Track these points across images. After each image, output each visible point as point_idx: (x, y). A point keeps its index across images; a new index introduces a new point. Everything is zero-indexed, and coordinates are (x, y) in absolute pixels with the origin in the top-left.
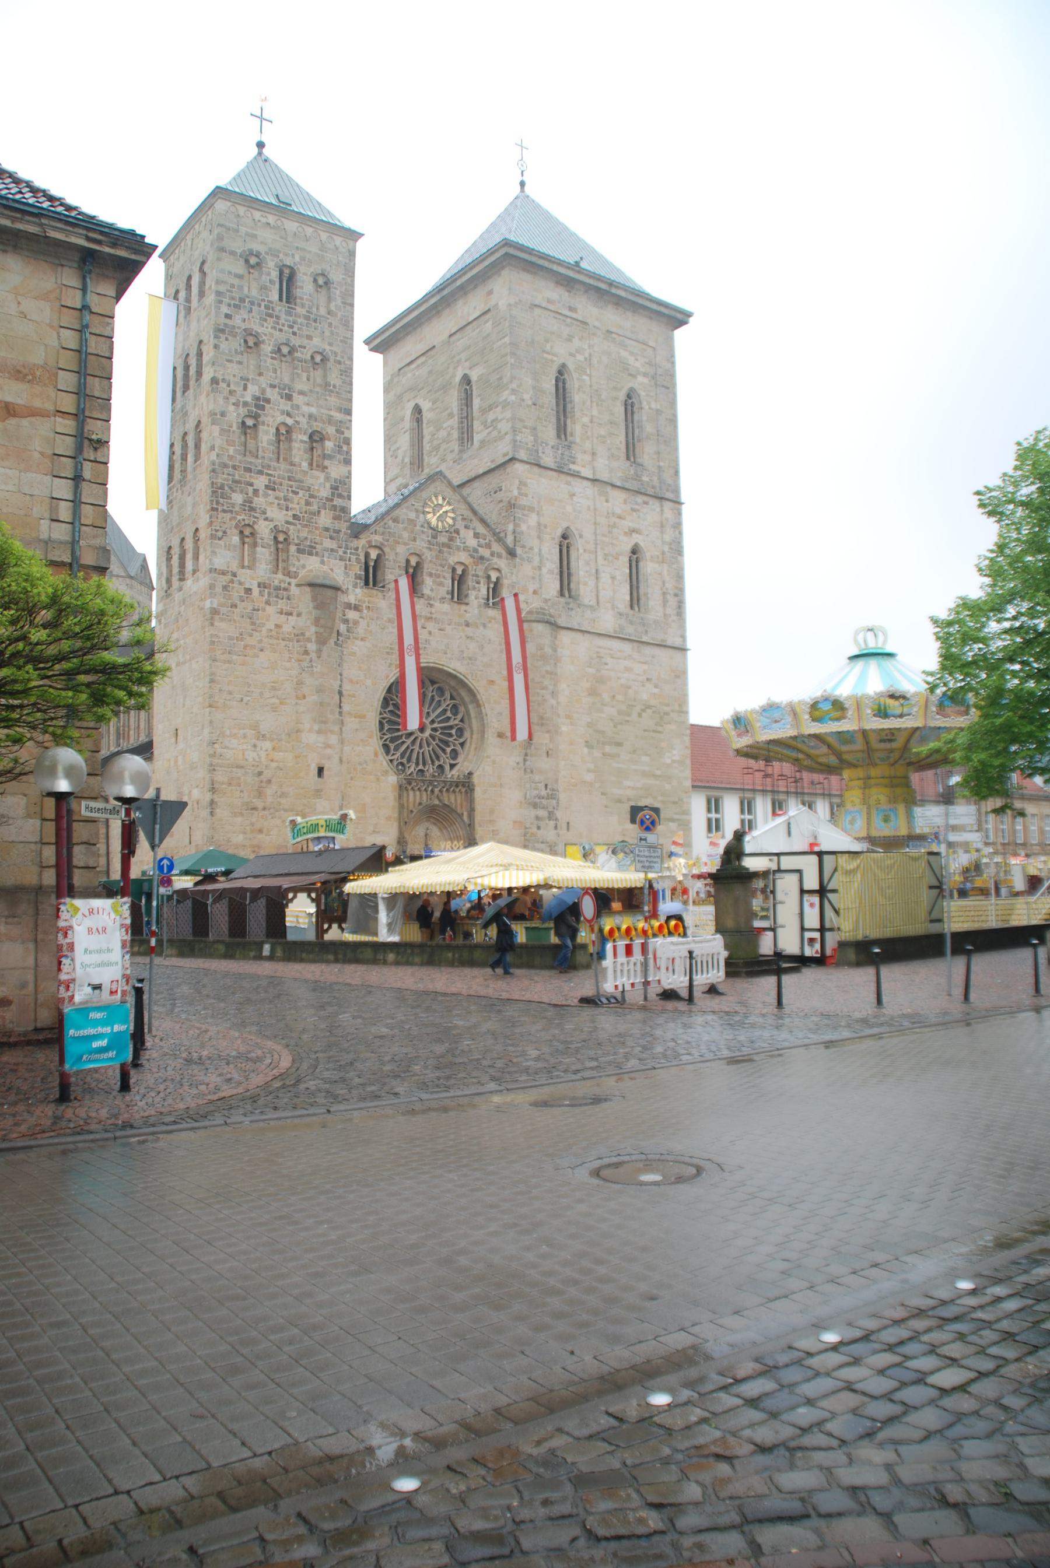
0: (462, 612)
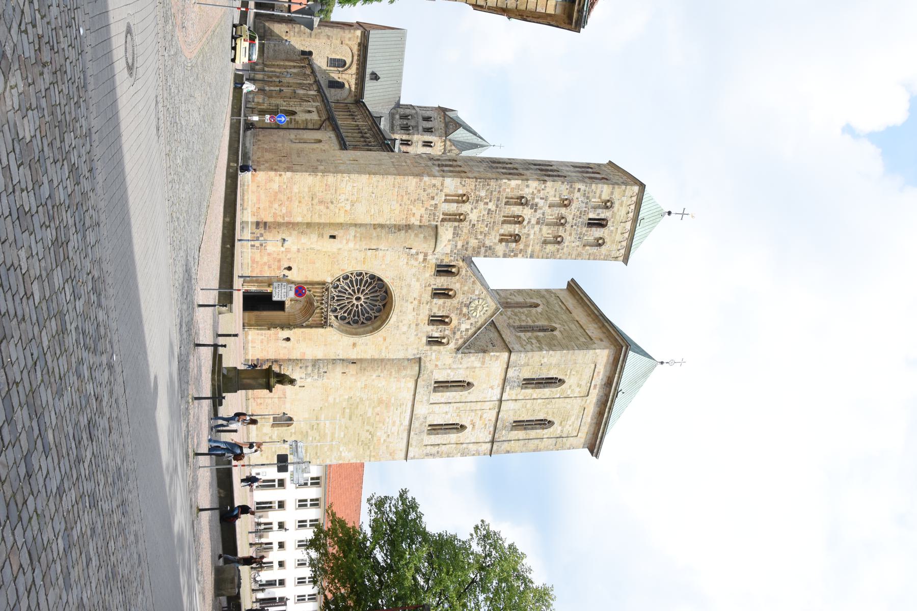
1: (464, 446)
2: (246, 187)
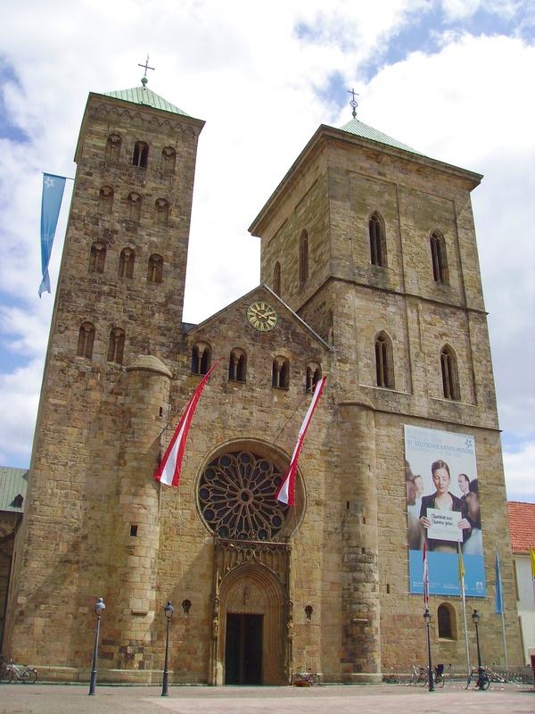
1: (474, 348)
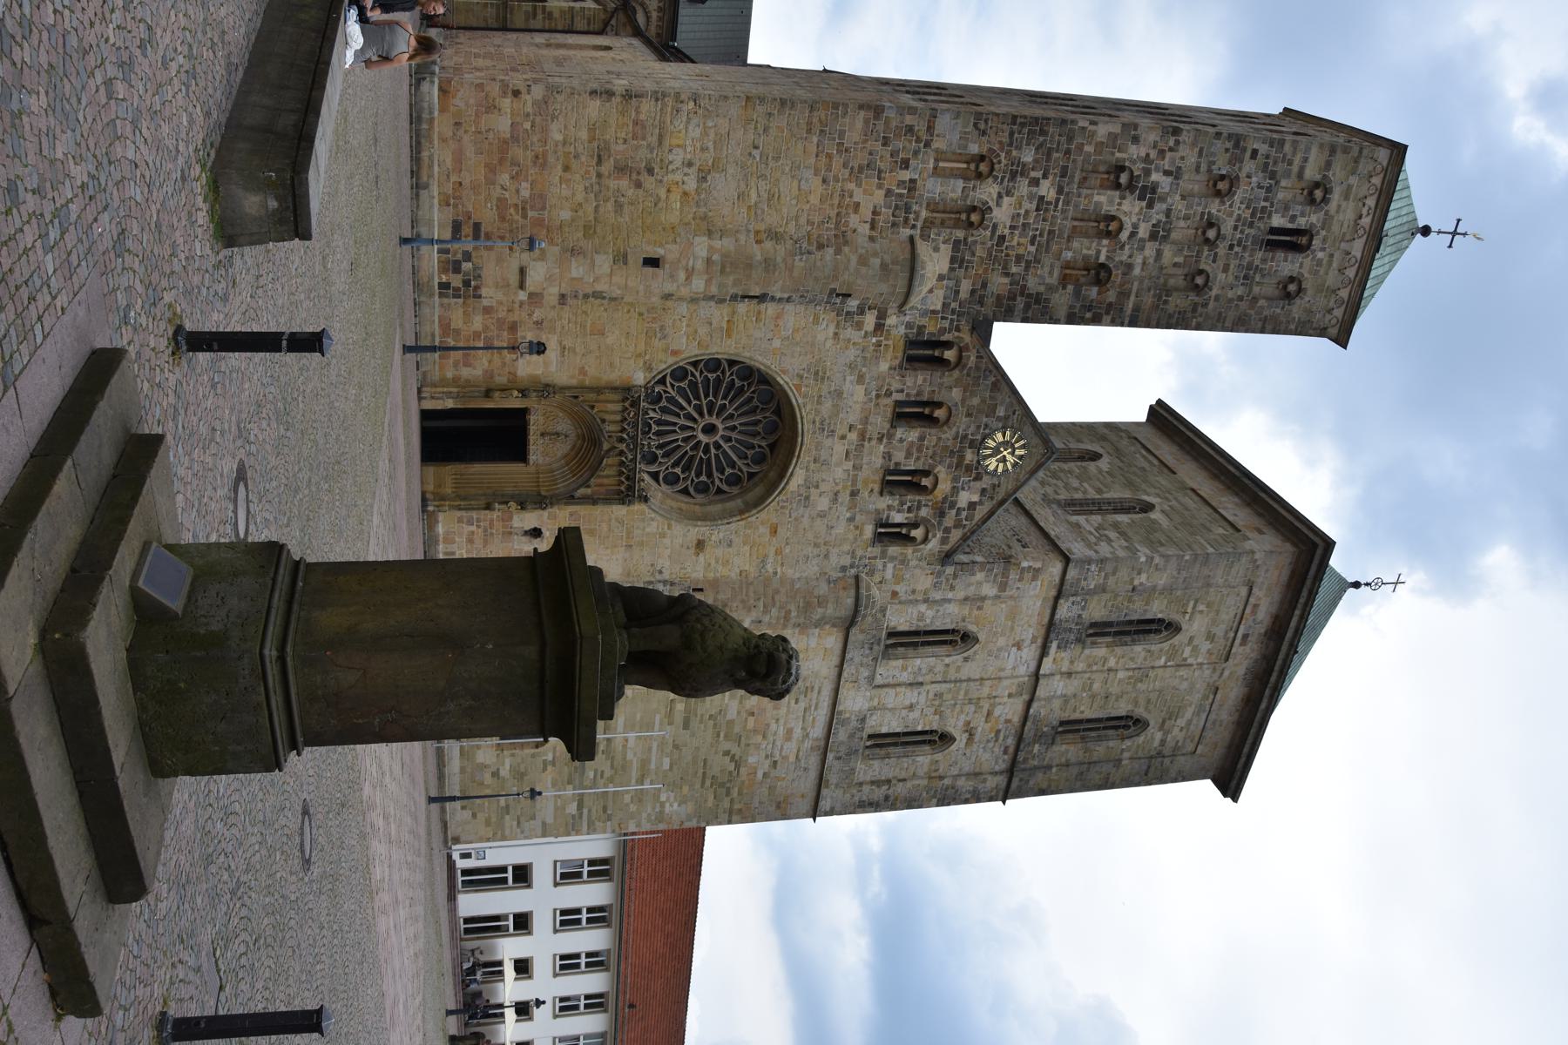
0: (871, 486)
2: (425, 126)
